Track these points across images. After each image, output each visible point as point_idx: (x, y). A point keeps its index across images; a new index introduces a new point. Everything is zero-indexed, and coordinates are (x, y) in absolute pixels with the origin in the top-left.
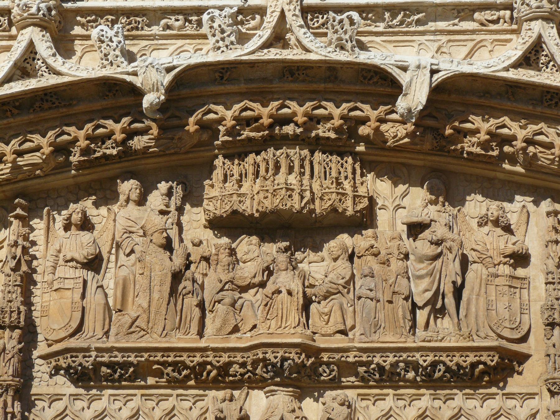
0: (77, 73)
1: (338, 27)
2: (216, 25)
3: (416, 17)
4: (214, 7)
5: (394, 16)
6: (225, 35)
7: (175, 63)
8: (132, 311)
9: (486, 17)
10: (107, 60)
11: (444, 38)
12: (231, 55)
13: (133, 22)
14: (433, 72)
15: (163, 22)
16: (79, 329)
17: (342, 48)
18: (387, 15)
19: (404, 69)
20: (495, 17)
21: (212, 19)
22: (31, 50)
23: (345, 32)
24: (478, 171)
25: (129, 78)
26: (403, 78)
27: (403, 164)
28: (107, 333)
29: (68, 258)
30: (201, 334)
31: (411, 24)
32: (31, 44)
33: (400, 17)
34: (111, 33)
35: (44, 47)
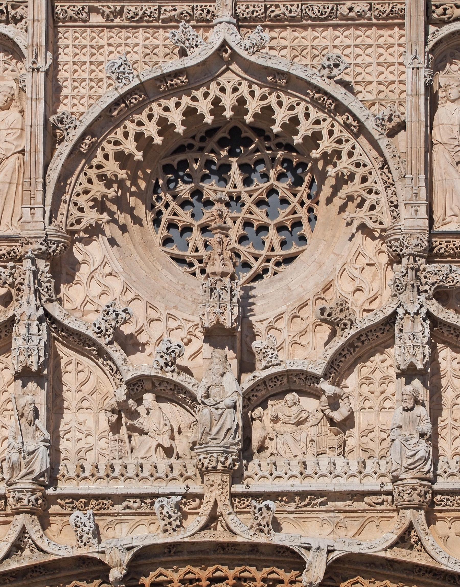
0: (60, 553)
1: (258, 514)
2: (164, 512)
3: (320, 500)
5: (302, 500)
6: (172, 519)
7: (134, 544)
9: (373, 501)
10: (82, 542)
11: (342, 515)
12: (176, 538)
13: (101, 504)
14: (329, 552)
15: (125, 504)
17: (261, 531)
18: (297, 498)
20: (380, 501)
21: (162, 507)
31: (316, 505)
33: (307, 501)
35: (34, 531)
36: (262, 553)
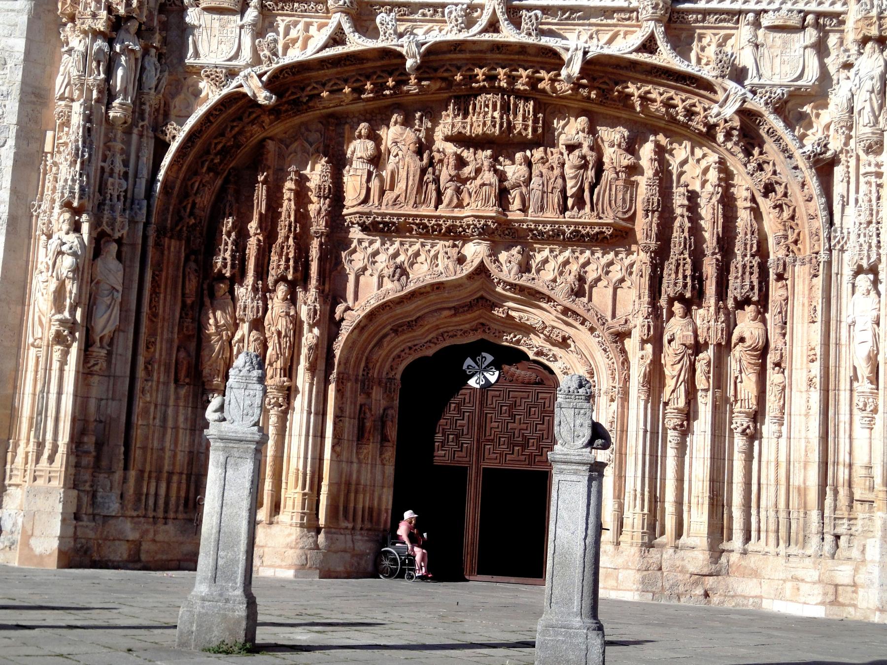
4: (453, 4)
5: (564, 14)
8: (397, 191)
12: (462, 36)
15: (421, 11)
16: (366, 201)
19: (567, 50)
20: (627, 16)
21: (451, 12)
22: (339, 29)
23: (533, 25)
24: (611, 113)
25: (399, 49)
26: (566, 57)
27: (565, 106)
28: (380, 204)
29: (359, 156)
30: (436, 208)
32: (339, 24)
33: (567, 14)
34: (388, 19)
35: (347, 27)
36: (529, 54)
